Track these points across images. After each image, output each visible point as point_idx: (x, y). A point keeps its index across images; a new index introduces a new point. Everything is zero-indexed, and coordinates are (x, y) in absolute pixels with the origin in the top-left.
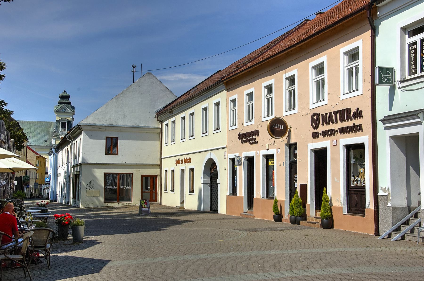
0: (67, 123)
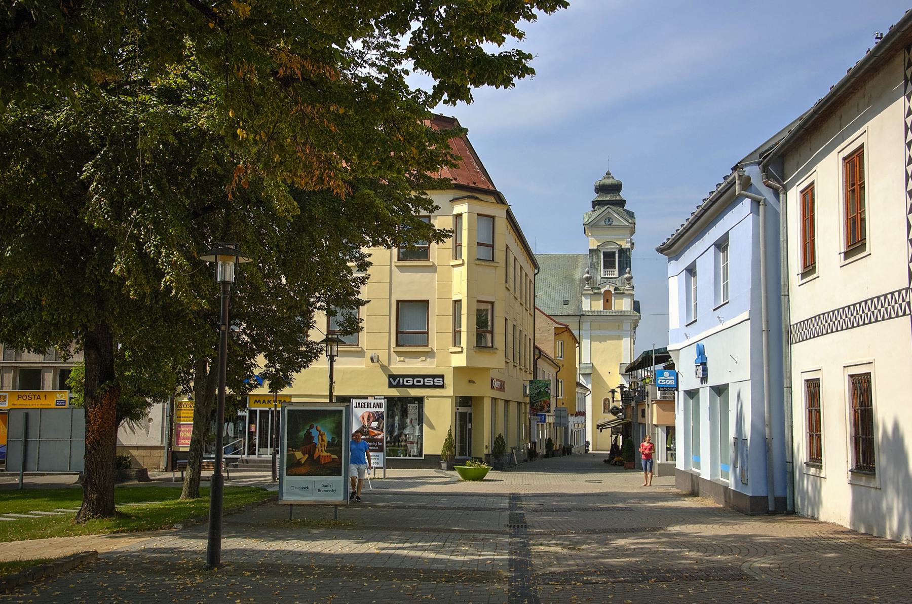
0: (617, 255)
